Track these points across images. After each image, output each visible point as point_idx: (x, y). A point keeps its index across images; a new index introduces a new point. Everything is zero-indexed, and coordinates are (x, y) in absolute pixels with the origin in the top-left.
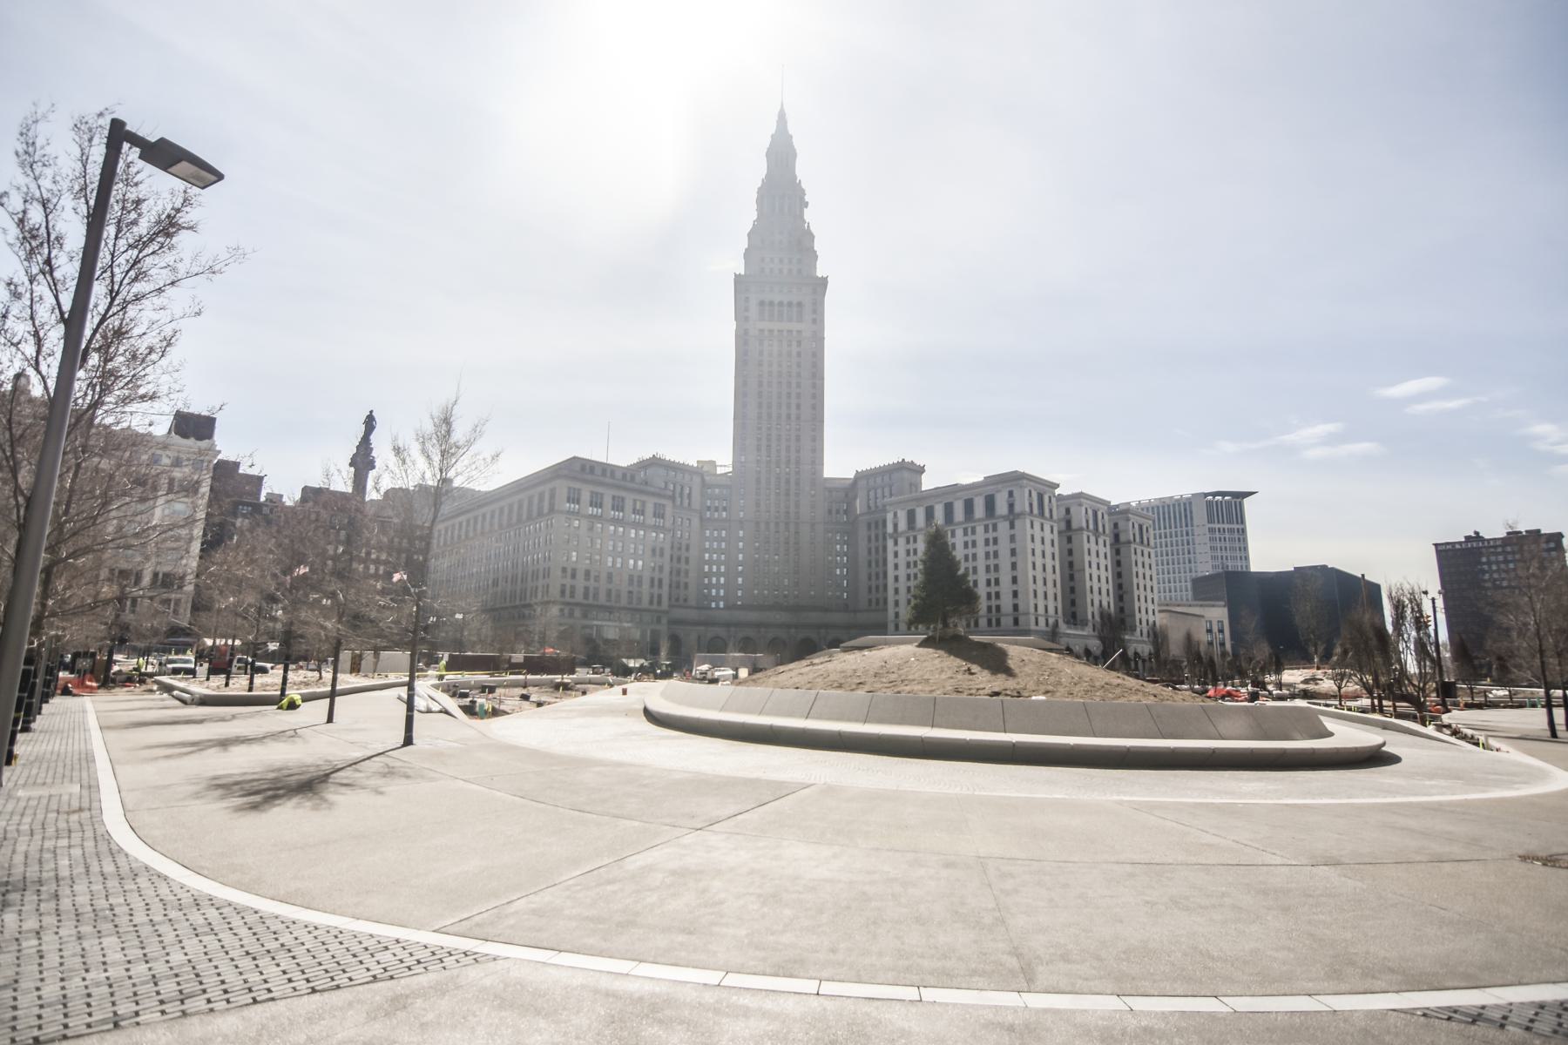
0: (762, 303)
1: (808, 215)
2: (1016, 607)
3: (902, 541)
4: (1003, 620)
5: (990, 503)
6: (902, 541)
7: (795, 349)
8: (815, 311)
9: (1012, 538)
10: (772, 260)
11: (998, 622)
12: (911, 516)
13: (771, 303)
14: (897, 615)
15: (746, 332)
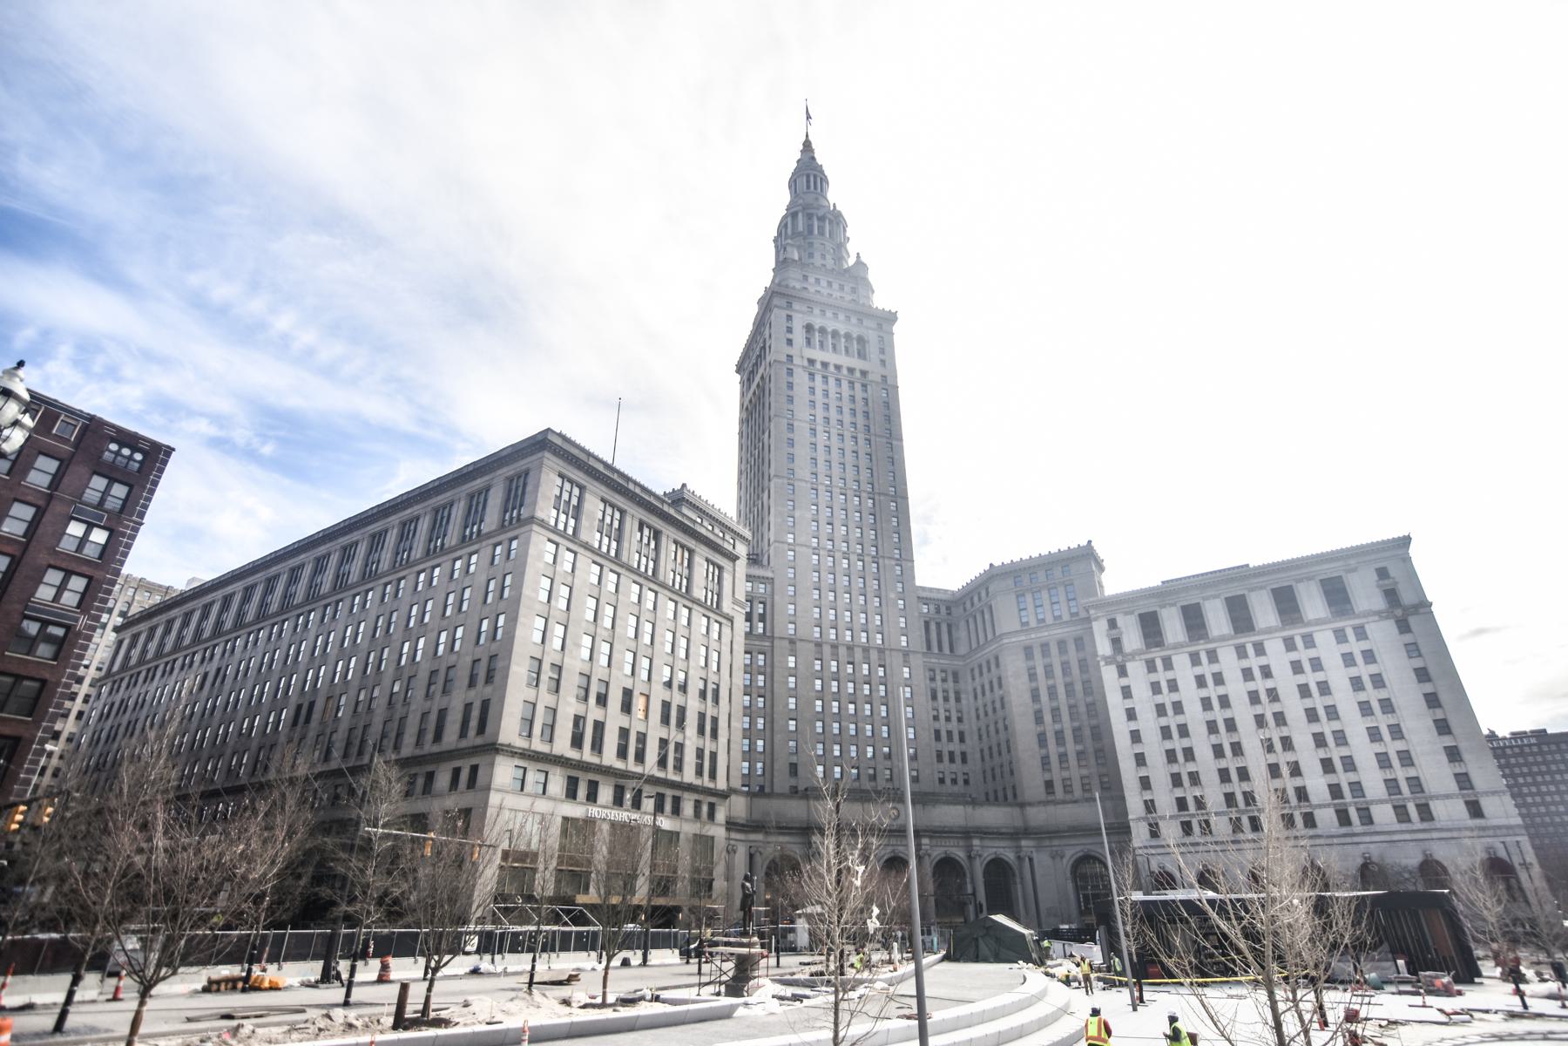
0: (809, 328)
1: (852, 248)
2: (1463, 780)
3: (1136, 669)
4: (1437, 808)
5: (1337, 595)
6: (1136, 669)
7: (859, 394)
8: (882, 351)
9: (1413, 650)
10: (818, 281)
11: (1425, 812)
12: (1151, 627)
13: (822, 330)
14: (1150, 806)
15: (790, 357)
